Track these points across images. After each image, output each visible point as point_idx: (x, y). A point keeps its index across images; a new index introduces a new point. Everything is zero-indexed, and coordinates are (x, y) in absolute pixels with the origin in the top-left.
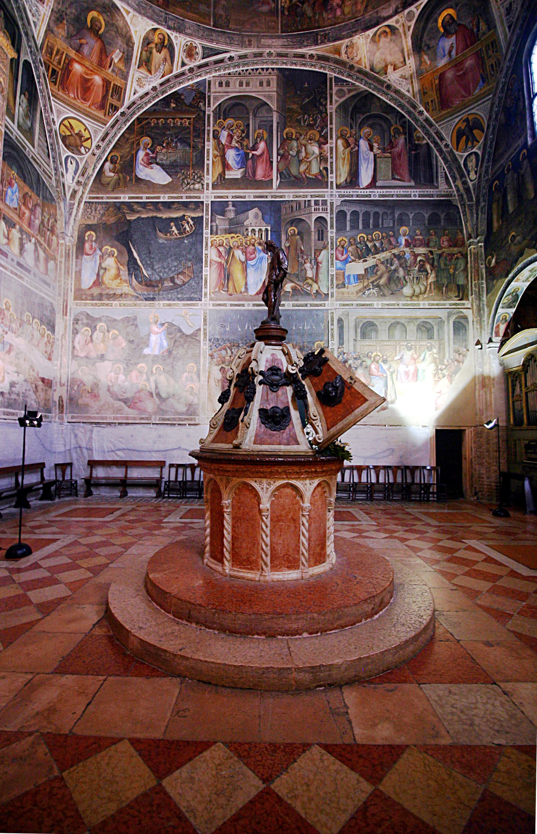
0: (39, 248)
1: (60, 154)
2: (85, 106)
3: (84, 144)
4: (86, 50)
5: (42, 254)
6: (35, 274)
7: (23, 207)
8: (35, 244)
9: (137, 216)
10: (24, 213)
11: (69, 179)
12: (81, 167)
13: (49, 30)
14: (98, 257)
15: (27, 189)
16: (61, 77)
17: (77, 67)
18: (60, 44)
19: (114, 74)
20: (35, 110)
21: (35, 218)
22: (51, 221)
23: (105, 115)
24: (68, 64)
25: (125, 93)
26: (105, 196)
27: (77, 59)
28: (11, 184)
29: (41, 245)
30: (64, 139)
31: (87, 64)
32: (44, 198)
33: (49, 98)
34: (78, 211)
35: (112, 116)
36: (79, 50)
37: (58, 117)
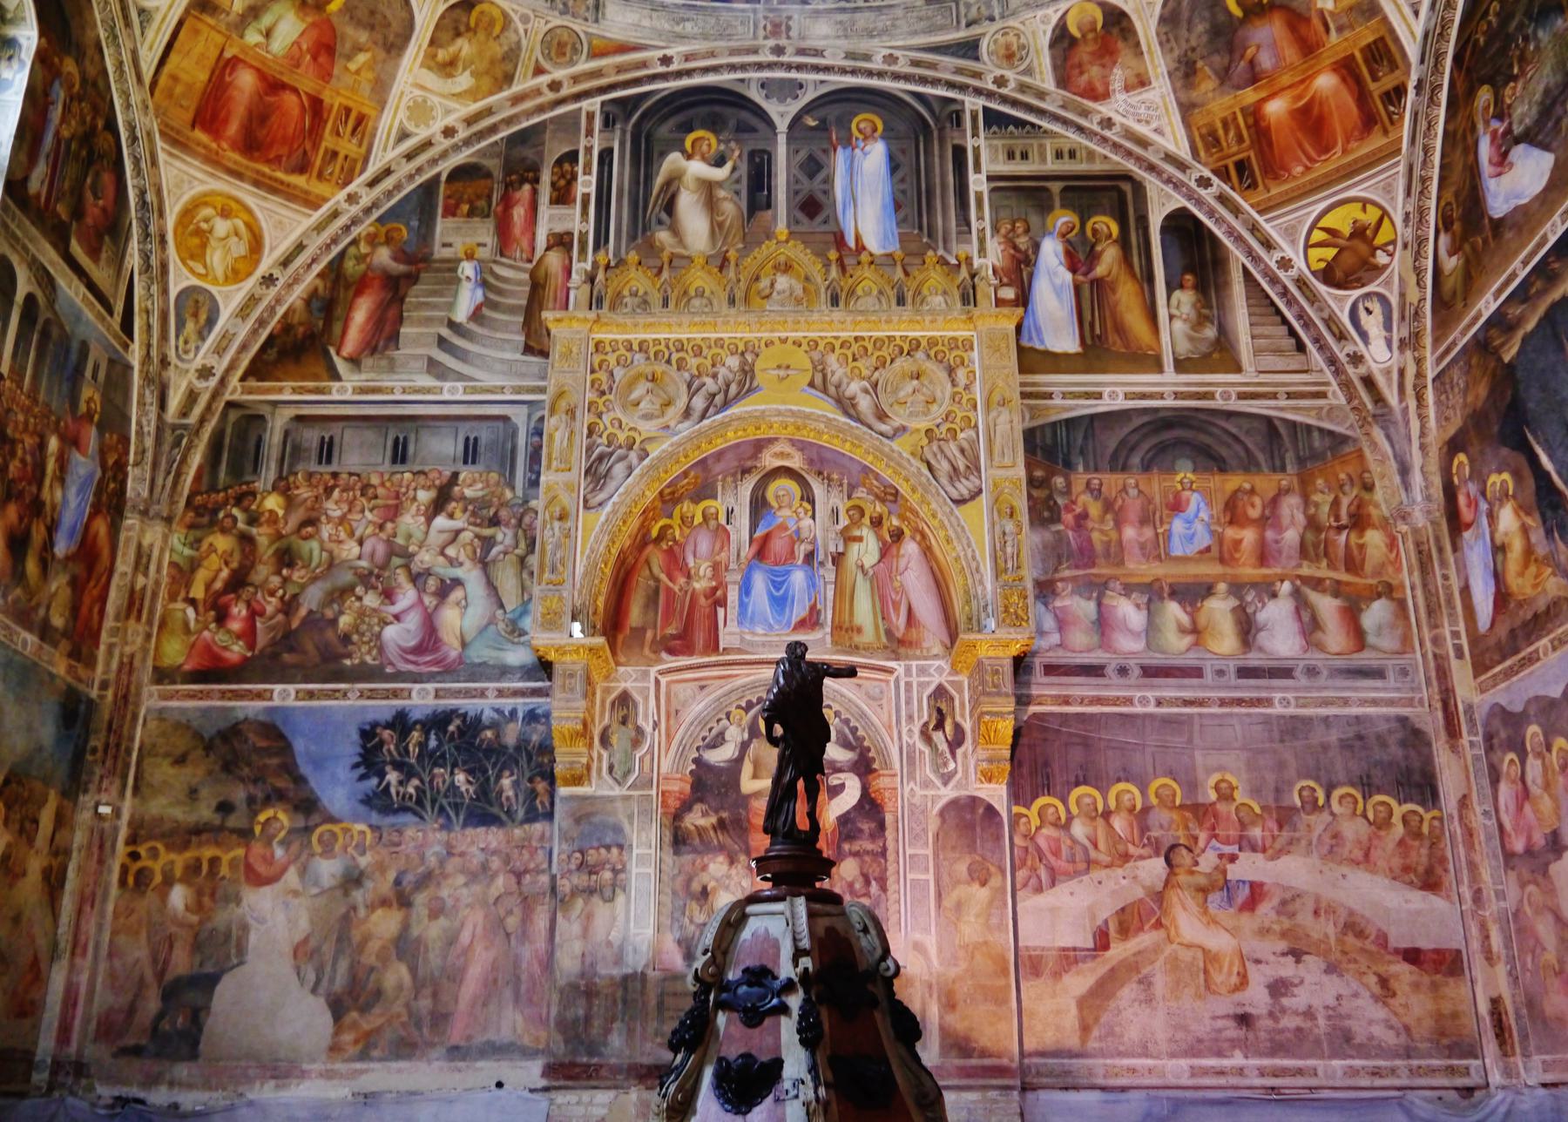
0: (1314, 597)
1: (1331, 321)
2: (1336, 159)
3: (1380, 239)
4: (1266, 61)
5: (1327, 606)
6: (1312, 672)
7: (1231, 533)
8: (1296, 594)
9: (1520, 334)
10: (1237, 543)
11: (1379, 355)
12: (1394, 300)
13: (1186, 109)
14: (1484, 521)
15: (1234, 481)
16: (1253, 160)
17: (1276, 108)
18: (1220, 104)
19: (1347, 34)
20: (1222, 286)
21: (1279, 528)
22: (1345, 502)
23: (1386, 132)
24: (1256, 122)
25: (1397, 40)
26: (1456, 333)
27: (1263, 94)
28: (1177, 506)
29: (1317, 584)
30: (1328, 275)
31: (1286, 80)
32: (1301, 461)
33: (1254, 228)
34: (1422, 418)
35: (1402, 118)
36: (1254, 77)
37: (1293, 242)
